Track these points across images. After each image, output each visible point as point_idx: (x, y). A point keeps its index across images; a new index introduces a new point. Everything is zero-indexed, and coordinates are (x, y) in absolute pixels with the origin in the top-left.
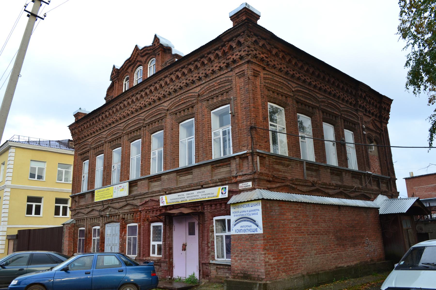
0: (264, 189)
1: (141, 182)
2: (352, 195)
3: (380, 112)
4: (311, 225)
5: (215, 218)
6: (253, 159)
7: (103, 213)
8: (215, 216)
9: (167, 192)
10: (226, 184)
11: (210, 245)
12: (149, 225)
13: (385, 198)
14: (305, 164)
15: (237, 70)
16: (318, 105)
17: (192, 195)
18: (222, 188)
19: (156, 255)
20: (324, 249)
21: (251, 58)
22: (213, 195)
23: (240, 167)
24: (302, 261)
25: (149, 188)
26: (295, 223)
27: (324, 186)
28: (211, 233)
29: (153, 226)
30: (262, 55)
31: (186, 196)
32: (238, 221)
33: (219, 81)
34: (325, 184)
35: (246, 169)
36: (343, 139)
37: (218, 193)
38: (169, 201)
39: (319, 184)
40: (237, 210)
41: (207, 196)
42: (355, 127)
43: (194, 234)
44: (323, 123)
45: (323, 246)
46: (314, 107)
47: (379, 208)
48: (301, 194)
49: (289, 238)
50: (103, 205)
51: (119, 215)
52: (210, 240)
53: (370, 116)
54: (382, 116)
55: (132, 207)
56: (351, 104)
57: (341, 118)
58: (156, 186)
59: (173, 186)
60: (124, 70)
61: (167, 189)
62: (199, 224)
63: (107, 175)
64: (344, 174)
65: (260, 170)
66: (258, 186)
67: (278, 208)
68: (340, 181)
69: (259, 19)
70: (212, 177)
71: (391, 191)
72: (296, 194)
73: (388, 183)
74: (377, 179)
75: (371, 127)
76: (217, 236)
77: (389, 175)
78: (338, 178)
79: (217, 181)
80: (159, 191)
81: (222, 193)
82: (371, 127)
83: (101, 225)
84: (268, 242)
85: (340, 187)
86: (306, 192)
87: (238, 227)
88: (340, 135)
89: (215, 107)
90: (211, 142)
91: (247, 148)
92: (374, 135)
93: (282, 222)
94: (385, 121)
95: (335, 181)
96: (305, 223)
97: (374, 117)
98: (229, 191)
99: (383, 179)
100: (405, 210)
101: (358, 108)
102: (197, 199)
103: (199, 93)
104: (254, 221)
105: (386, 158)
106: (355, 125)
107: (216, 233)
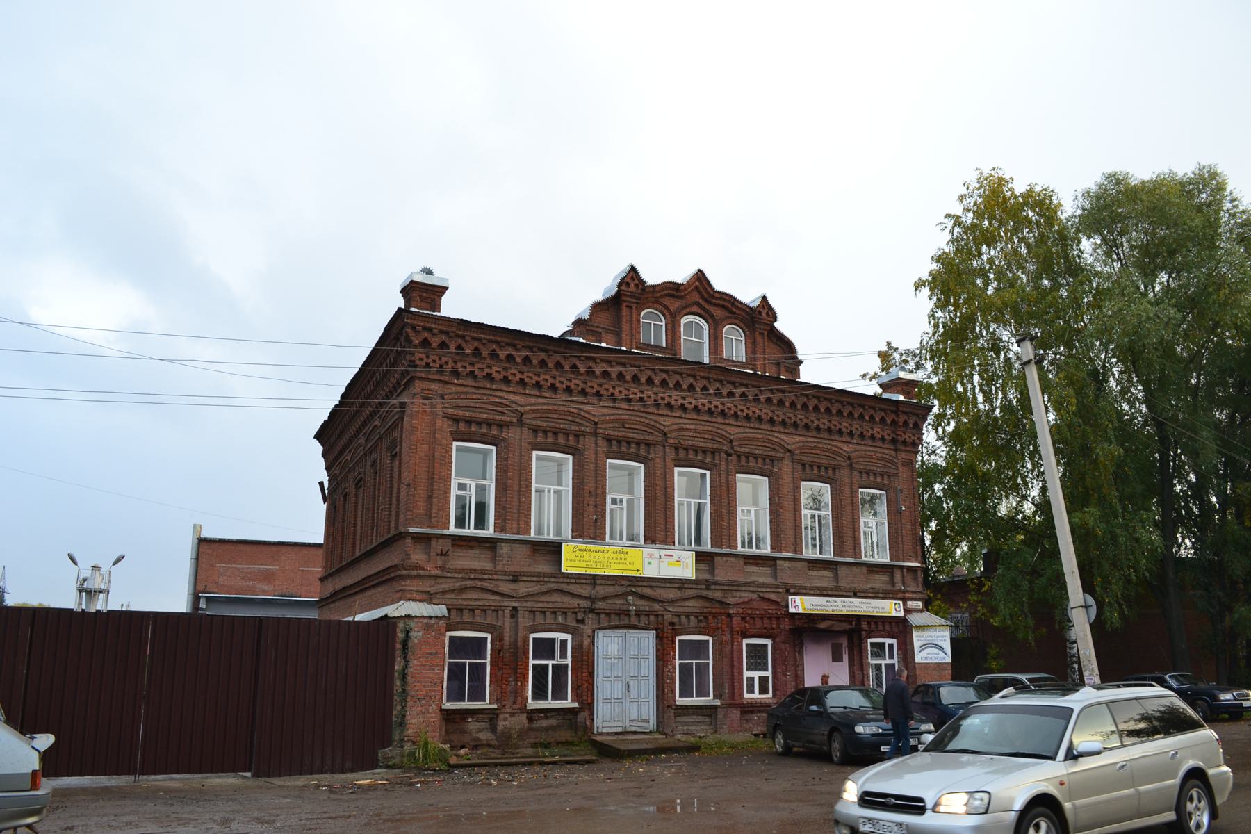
5: (870, 641)
19: (756, 695)
31: (840, 605)
32: (923, 647)
38: (807, 606)
40: (921, 633)
43: (841, 660)
50: (594, 584)
55: (707, 604)
61: (793, 586)
87: (924, 653)
104: (942, 649)
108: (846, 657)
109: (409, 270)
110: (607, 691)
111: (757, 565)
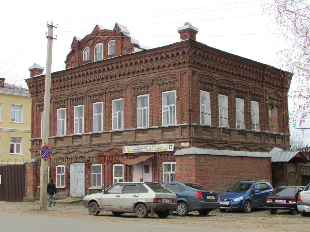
0: (196, 147)
1: (105, 135)
2: (252, 148)
3: (282, 84)
4: (222, 169)
5: (163, 163)
6: (190, 129)
7: (68, 156)
8: (163, 162)
9: (128, 144)
10: (172, 143)
11: (160, 179)
12: (112, 166)
13: (279, 149)
14: (221, 130)
15: (182, 70)
16: (233, 87)
17: (148, 148)
18: (170, 145)
20: (230, 183)
21: (191, 64)
22: (164, 149)
23: (182, 132)
24: (216, 189)
25: (111, 140)
26: (213, 167)
27: (233, 143)
28: (160, 173)
29: (115, 167)
30: (198, 61)
33: (169, 74)
34: (234, 142)
35: (186, 133)
36: (250, 109)
37: (166, 147)
38: (130, 150)
39: (230, 142)
41: (159, 149)
42: (260, 98)
44: (236, 98)
45: (229, 182)
46: (230, 89)
47: (271, 158)
48: (217, 149)
49: (209, 176)
51: (84, 158)
52: (161, 176)
53: (274, 88)
54: (284, 87)
56: (259, 81)
57: (249, 94)
58: (117, 139)
59: (133, 140)
60: (85, 42)
62: (152, 166)
63: (70, 126)
64: (248, 134)
65: (194, 135)
66: (193, 145)
67: (204, 159)
68: (245, 139)
69: (197, 33)
70: (162, 137)
71: (285, 144)
72: (214, 149)
73: (283, 138)
74: (274, 136)
75: (274, 96)
76: (164, 174)
77: (284, 133)
78: (244, 137)
79: (166, 140)
80: (121, 143)
81: (170, 148)
82: (274, 96)
83: (67, 164)
84: (197, 178)
85: (244, 143)
86: (221, 148)
88: (247, 106)
89: (165, 90)
90: (162, 113)
91: (187, 122)
92: (275, 102)
93: (206, 166)
94: (286, 91)
95: (242, 139)
96: (219, 168)
97: (276, 88)
98: (174, 147)
99: (279, 135)
100: (287, 159)
101: (264, 84)
102: (152, 150)
103: (154, 78)
105: (284, 119)
106: (260, 97)
107: (164, 172)
108: (151, 171)
109: (31, 66)
110: (73, 183)
111: (117, 135)
